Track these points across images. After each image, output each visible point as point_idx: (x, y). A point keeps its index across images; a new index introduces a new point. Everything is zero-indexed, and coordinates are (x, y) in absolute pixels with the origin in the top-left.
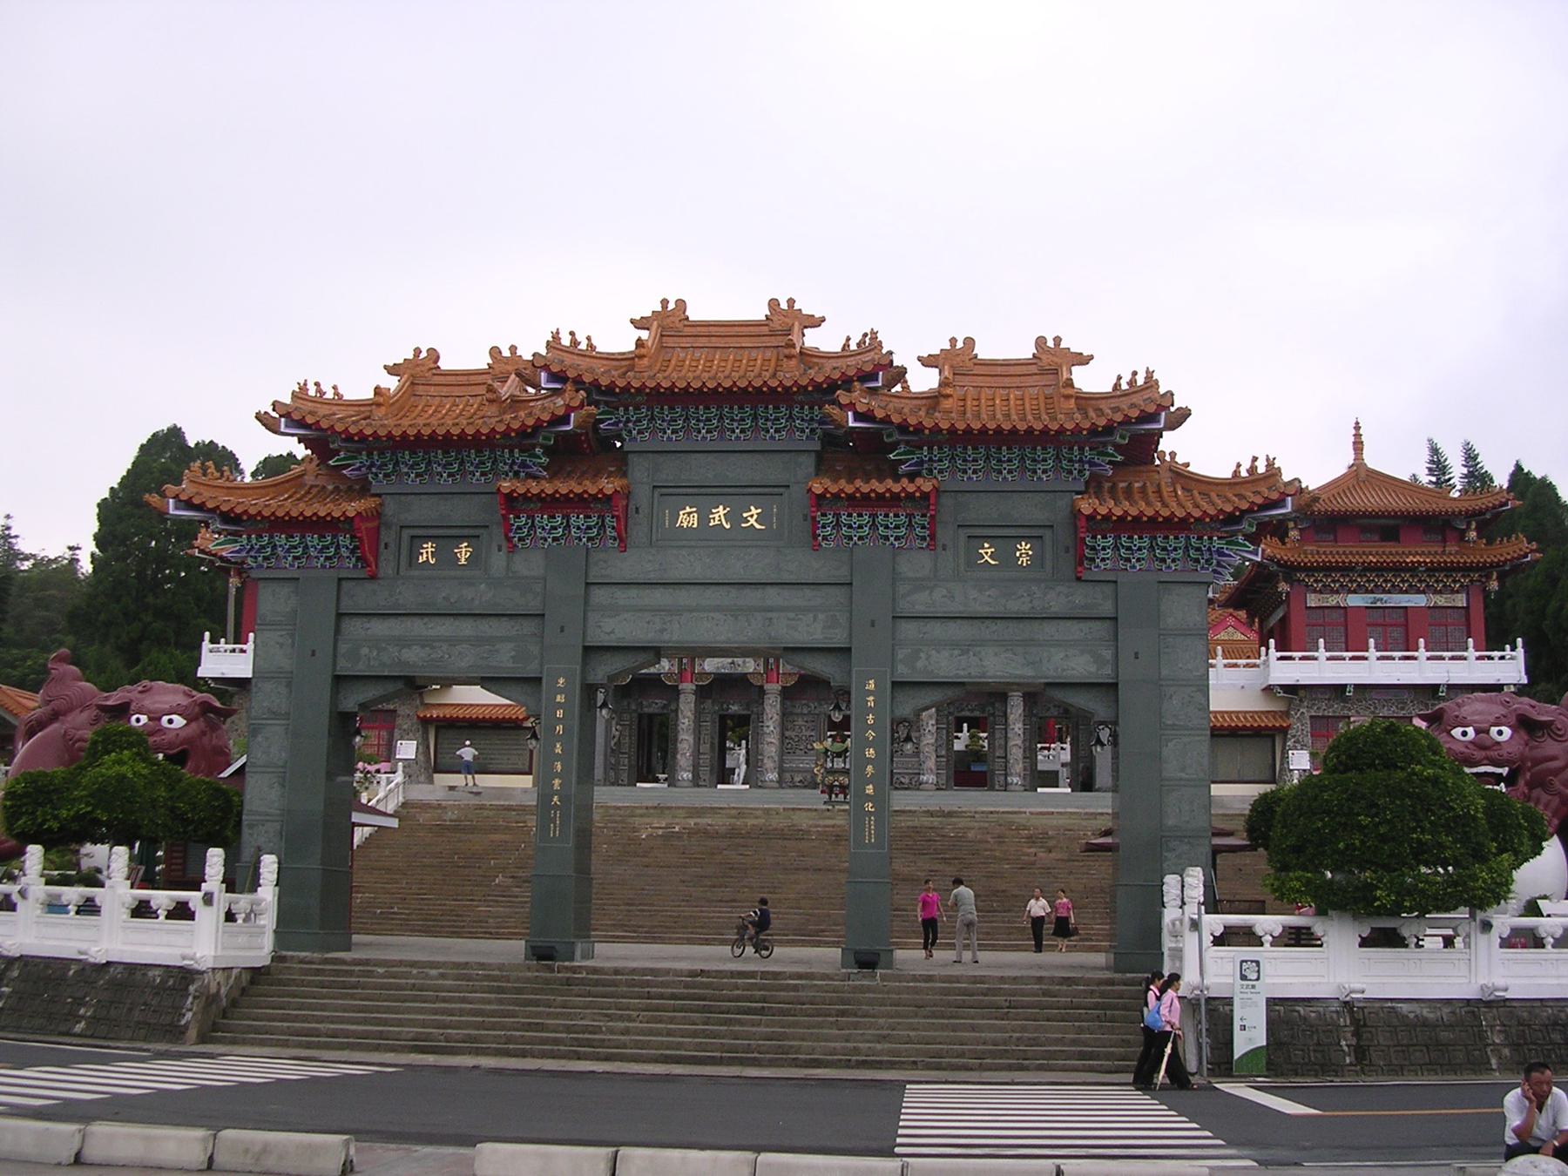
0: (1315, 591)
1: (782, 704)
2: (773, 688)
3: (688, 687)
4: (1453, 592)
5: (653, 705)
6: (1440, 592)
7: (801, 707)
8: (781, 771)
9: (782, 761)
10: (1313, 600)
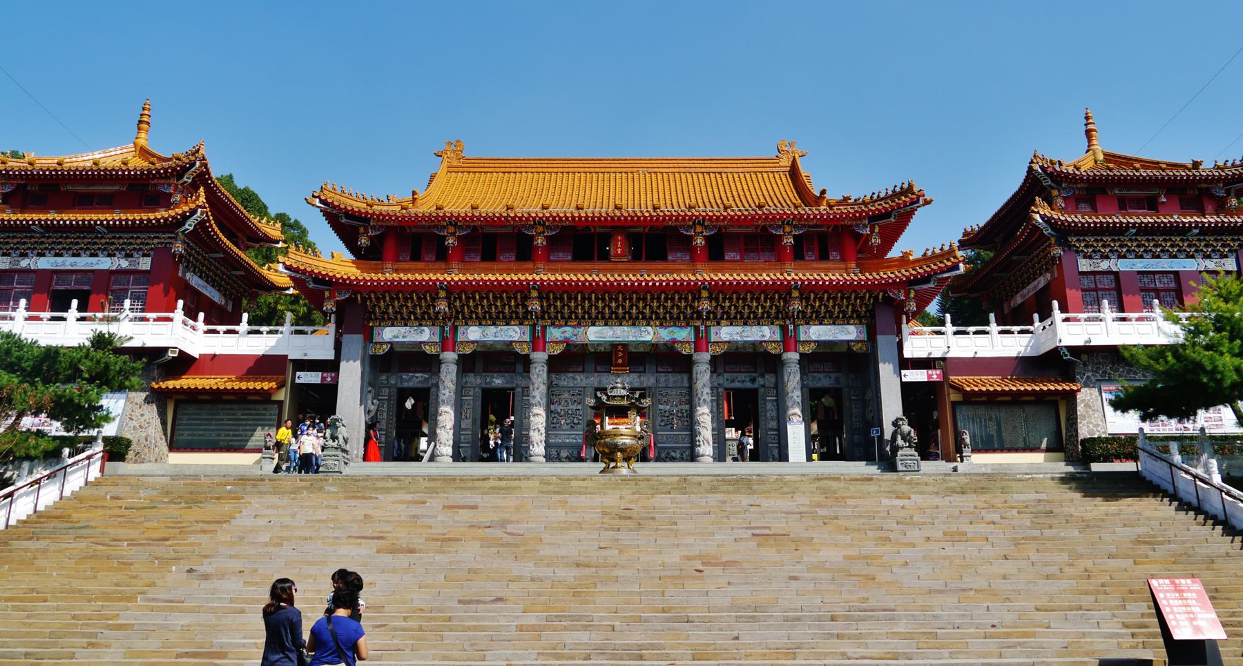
0: (1085, 257)
1: (549, 377)
2: (540, 357)
3: (450, 356)
4: (1224, 256)
5: (416, 379)
6: (1209, 257)
7: (566, 380)
10: (1084, 265)
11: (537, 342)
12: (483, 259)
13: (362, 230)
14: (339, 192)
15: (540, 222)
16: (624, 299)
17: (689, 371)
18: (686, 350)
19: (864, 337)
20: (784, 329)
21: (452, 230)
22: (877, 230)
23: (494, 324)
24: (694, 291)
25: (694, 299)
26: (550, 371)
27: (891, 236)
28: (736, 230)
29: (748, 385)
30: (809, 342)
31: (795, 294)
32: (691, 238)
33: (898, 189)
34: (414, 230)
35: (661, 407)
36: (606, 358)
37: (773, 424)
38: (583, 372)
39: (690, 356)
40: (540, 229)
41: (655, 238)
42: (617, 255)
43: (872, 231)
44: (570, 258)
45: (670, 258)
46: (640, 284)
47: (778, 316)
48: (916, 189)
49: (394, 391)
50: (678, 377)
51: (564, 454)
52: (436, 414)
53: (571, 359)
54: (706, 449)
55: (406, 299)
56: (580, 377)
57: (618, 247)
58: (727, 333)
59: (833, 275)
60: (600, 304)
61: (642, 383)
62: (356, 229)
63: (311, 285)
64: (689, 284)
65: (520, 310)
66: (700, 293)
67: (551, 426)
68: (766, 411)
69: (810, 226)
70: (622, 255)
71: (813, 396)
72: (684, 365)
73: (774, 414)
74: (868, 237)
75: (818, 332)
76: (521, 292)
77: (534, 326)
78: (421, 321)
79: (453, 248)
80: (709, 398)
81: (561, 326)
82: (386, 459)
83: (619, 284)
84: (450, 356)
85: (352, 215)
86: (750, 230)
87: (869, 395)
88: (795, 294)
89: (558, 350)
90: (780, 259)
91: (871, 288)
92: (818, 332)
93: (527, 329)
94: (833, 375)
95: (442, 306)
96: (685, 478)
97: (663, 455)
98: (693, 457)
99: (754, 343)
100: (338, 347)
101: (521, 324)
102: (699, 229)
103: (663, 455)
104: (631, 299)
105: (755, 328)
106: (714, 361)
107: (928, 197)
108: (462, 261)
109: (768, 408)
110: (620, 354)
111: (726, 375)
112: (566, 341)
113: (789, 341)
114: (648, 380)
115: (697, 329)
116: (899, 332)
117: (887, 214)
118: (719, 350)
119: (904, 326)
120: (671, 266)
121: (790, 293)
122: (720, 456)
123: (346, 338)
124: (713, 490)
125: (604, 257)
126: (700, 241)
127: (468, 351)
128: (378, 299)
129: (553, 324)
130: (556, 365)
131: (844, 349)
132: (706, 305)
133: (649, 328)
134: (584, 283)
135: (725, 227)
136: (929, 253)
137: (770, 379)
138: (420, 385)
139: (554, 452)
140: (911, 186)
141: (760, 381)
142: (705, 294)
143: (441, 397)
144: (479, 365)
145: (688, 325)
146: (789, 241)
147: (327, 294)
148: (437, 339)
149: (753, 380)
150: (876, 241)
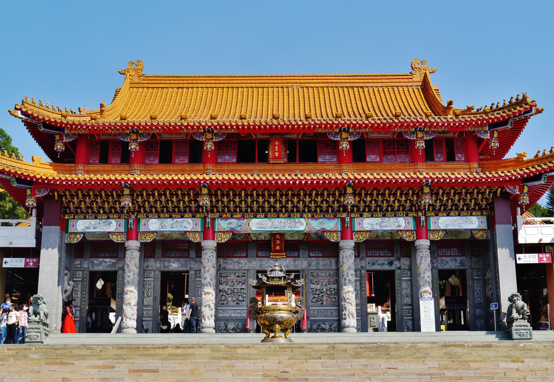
1: (217, 262)
2: (210, 245)
5: (104, 264)
7: (232, 264)
8: (217, 320)
9: (217, 311)
11: (207, 232)
12: (162, 162)
13: (57, 137)
14: (37, 104)
15: (209, 130)
16: (281, 195)
17: (337, 256)
18: (334, 238)
19: (485, 226)
20: (417, 220)
21: (134, 137)
22: (496, 135)
23: (171, 217)
24: (340, 188)
25: (340, 195)
26: (219, 256)
27: (508, 140)
28: (376, 135)
29: (387, 267)
30: (438, 231)
31: (427, 190)
32: (337, 143)
33: (514, 101)
34: (102, 137)
35: (312, 286)
36: (266, 245)
37: (408, 300)
38: (247, 257)
39: (338, 243)
40: (209, 136)
41: (307, 144)
42: (274, 158)
43: (492, 136)
44: (234, 160)
45: (320, 160)
46: (294, 183)
47: (413, 209)
48: (529, 100)
49: (87, 273)
50: (327, 261)
51: (231, 326)
52: (123, 293)
53: (236, 246)
54: (351, 321)
55: (96, 196)
56: (243, 261)
57: (275, 150)
58: (369, 224)
59: (459, 172)
60: (261, 199)
61: (296, 266)
62: (53, 137)
63: (15, 185)
64: (336, 182)
65: (193, 205)
66: (346, 190)
67: (220, 303)
68: (402, 290)
69: (439, 132)
70: (279, 157)
71: (442, 275)
72: (332, 250)
73: (409, 292)
74: (488, 142)
75: (445, 223)
76: (193, 189)
77: (205, 218)
78: (108, 214)
79: (136, 152)
80: (353, 279)
81: (228, 218)
82: (80, 331)
83: (277, 183)
84: (133, 244)
85: (48, 124)
86: (389, 136)
87: (489, 275)
88: (427, 190)
89: (225, 238)
90: (414, 160)
91: (490, 184)
92: (445, 223)
93: (199, 221)
94: (458, 259)
95: (127, 202)
96: (333, 346)
97: (315, 327)
98: (340, 328)
99: (391, 232)
100: (39, 236)
101: (194, 217)
102: (344, 135)
103: (315, 327)
104: (287, 195)
105: (392, 220)
106: (358, 247)
107: (539, 107)
108: (143, 163)
109: (403, 287)
110: (278, 242)
111: (368, 259)
112: (232, 231)
113: (421, 230)
114: (302, 263)
115: (343, 220)
116: (515, 221)
117: (505, 122)
118: (362, 238)
119: (519, 217)
120: (320, 167)
121: (422, 190)
122: (363, 327)
123: (45, 229)
124: (357, 355)
125: (264, 159)
126: (345, 146)
127: (149, 239)
128: (72, 196)
129: (221, 217)
130: (223, 251)
131: (468, 236)
132: (350, 200)
133: (302, 220)
134: (246, 182)
135: (367, 134)
136: (540, 155)
137: (405, 262)
138: (108, 269)
139: (222, 324)
140: (525, 98)
141: (397, 264)
142: (350, 190)
143: (127, 279)
144: (159, 252)
145: (335, 217)
146: (421, 145)
147: (29, 192)
148: (122, 229)
149: (391, 263)
150: (495, 144)
